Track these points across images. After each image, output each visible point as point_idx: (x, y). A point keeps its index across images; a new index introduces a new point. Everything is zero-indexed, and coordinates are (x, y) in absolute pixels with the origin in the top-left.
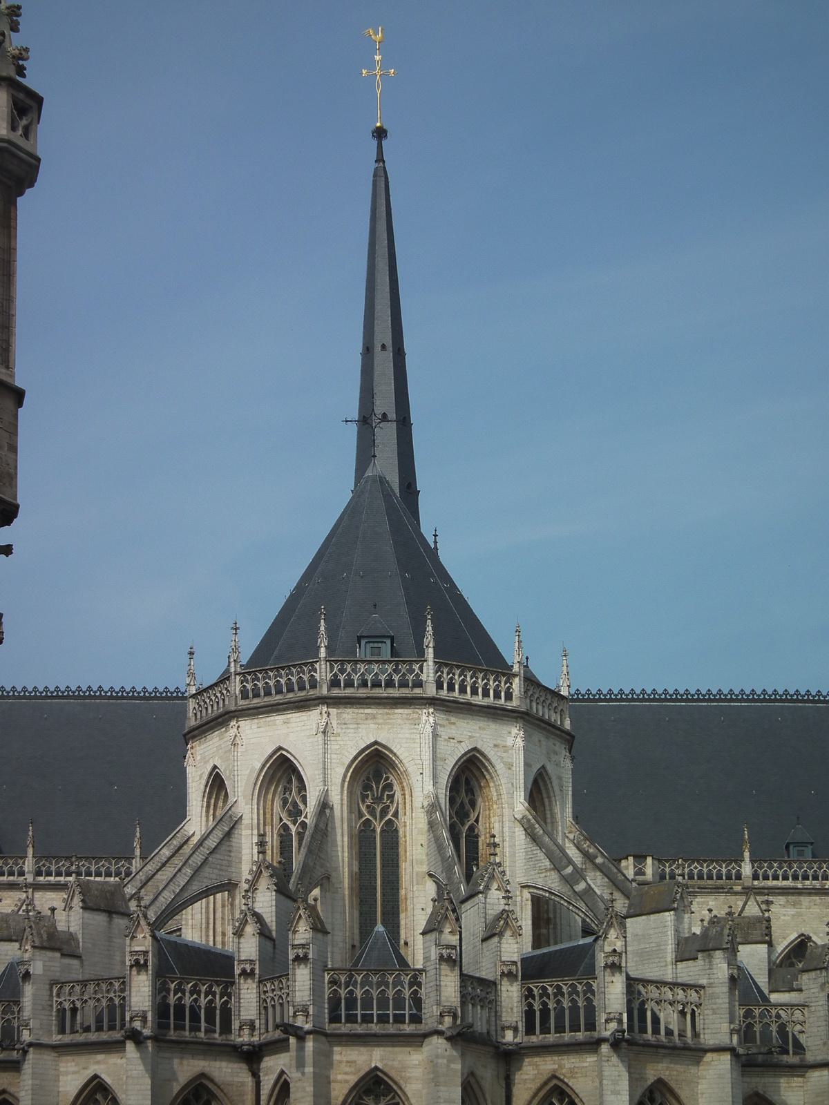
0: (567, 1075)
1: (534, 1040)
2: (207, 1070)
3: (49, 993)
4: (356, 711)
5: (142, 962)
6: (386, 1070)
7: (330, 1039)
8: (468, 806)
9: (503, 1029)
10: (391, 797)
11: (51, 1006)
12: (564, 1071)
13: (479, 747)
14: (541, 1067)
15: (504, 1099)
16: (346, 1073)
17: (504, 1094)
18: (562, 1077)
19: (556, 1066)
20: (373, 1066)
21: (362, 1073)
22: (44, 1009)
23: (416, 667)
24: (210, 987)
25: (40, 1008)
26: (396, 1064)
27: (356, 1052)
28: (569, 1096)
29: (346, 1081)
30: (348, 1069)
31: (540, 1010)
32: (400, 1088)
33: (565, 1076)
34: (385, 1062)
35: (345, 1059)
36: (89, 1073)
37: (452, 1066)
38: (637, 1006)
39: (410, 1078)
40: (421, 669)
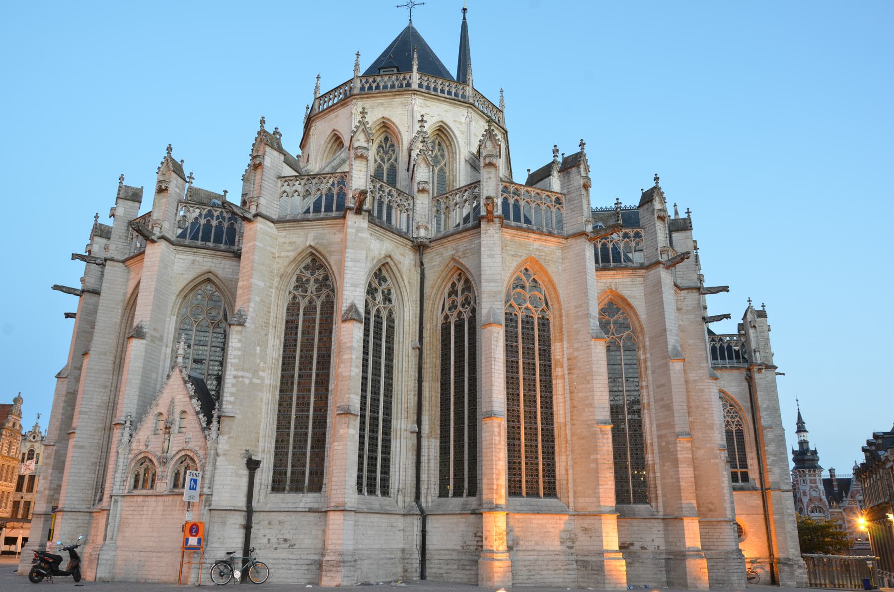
2: (213, 269)
5: (163, 187)
7: (278, 225)
8: (440, 157)
9: (418, 228)
10: (394, 151)
11: (127, 237)
12: (459, 254)
13: (444, 120)
14: (444, 255)
15: (419, 281)
16: (288, 251)
17: (419, 278)
19: (454, 252)
20: (308, 244)
21: (300, 250)
22: (120, 238)
23: (408, 77)
24: (221, 213)
25: (118, 237)
28: (465, 274)
29: (287, 257)
30: (290, 248)
32: (327, 260)
35: (288, 241)
37: (360, 234)
38: (513, 202)
40: (410, 78)
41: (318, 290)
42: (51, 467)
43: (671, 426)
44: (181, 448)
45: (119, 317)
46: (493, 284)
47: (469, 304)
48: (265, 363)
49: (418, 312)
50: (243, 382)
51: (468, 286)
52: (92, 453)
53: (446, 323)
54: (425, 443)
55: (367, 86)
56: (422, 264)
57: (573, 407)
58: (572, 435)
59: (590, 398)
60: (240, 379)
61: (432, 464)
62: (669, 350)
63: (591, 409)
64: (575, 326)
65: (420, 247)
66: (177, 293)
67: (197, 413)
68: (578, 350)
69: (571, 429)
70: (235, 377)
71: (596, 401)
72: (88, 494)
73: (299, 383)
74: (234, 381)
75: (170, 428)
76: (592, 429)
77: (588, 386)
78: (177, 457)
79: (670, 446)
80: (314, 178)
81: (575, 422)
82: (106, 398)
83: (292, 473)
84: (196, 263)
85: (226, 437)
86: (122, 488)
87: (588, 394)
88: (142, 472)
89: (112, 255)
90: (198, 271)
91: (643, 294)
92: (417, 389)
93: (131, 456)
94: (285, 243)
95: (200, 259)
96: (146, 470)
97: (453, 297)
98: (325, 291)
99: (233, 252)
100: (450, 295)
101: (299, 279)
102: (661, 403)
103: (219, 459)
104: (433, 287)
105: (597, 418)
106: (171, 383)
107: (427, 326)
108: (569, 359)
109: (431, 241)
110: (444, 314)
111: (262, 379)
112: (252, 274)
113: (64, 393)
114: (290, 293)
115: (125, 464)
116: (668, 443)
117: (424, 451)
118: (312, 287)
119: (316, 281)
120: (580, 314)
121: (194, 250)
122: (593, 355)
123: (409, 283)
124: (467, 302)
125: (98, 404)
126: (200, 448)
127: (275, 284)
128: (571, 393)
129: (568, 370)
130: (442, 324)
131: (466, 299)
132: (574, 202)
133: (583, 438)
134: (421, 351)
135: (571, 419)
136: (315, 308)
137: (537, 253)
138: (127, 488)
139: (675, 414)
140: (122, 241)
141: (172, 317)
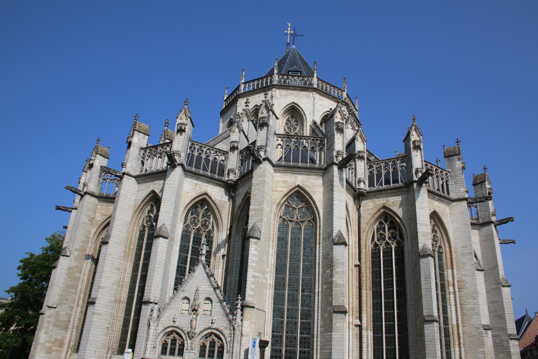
0: (391, 205)
1: (373, 189)
2: (209, 192)
3: (138, 153)
4: (286, 91)
6: (303, 187)
9: (359, 182)
16: (282, 187)
18: (388, 206)
19: (385, 201)
20: (297, 184)
21: (291, 188)
22: (135, 159)
26: (309, 184)
27: (288, 177)
29: (282, 191)
30: (283, 185)
31: (376, 174)
33: (390, 206)
34: (303, 183)
35: (282, 180)
36: (149, 190)
39: (316, 192)
42: (52, 325)
43: (505, 329)
44: (207, 327)
45: (130, 218)
46: (425, 227)
48: (268, 268)
49: (357, 240)
50: (258, 280)
52: (106, 320)
54: (364, 333)
55: (283, 80)
57: (463, 314)
58: (463, 333)
59: (476, 309)
60: (257, 279)
61: (370, 349)
62: (501, 279)
63: (478, 317)
64: (462, 260)
66: (185, 206)
67: (221, 302)
68: (465, 275)
69: (463, 330)
70: (254, 277)
71: (481, 312)
72: (101, 352)
73: (289, 285)
74: (253, 280)
75: (196, 310)
76: (479, 330)
77: (474, 301)
78: (204, 333)
79: (504, 343)
80: (293, 138)
81: (465, 325)
82: (118, 278)
83: (286, 351)
84: (198, 186)
85: (248, 322)
86: (152, 353)
87: (475, 306)
88: (169, 342)
89: (128, 171)
90: (199, 192)
91: (479, 241)
92: (358, 294)
93: (160, 328)
94: (279, 181)
95: (200, 183)
96: (174, 341)
99: (223, 182)
100: (378, 230)
102: (496, 313)
103: (243, 338)
104: (367, 224)
105: (482, 323)
106: (196, 276)
107: (363, 251)
108: (458, 282)
110: (374, 242)
111: (266, 279)
112: (263, 201)
113: (67, 267)
114: (281, 217)
115: (155, 334)
116: (501, 341)
117: (364, 339)
120: (466, 252)
121: (198, 176)
122: (477, 280)
123: (352, 219)
125: (113, 282)
126: (226, 328)
127: (274, 210)
128: (461, 304)
129: (458, 289)
130: (372, 250)
132: (457, 178)
133: (472, 336)
134: (359, 266)
135: (462, 323)
137: (438, 209)
138: (157, 353)
139: (507, 322)
140: (136, 161)
141: (180, 224)
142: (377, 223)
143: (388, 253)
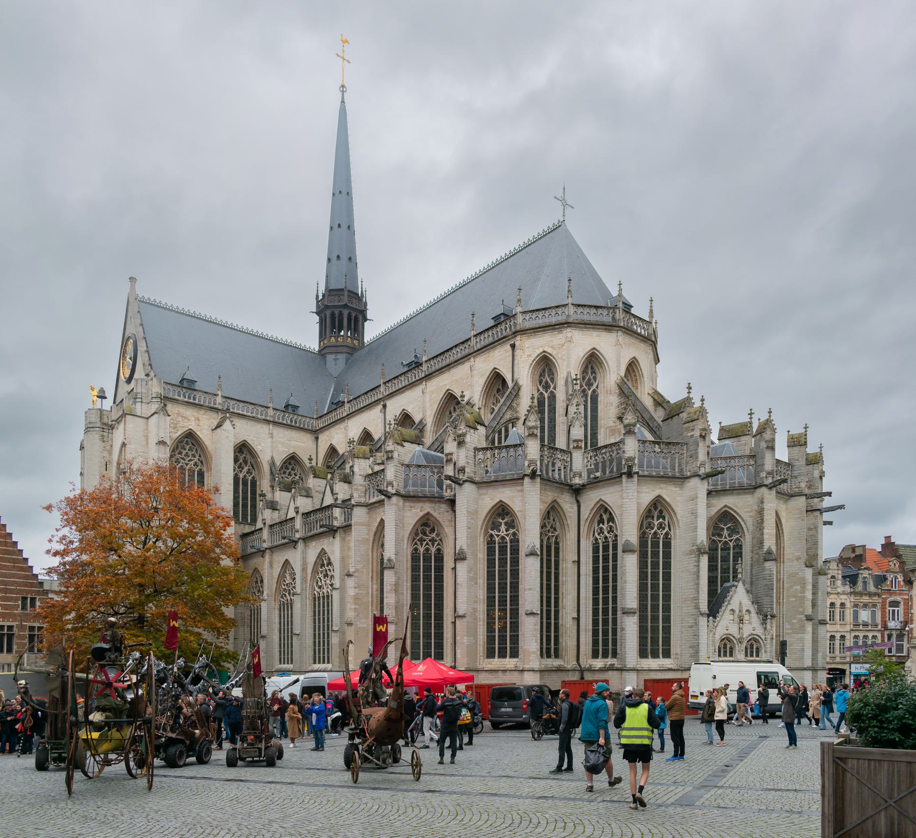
9: (574, 476)
41: (507, 531)
47: (613, 532)
51: (611, 519)
53: (596, 543)
56: (578, 502)
65: (577, 491)
97: (601, 525)
98: (511, 531)
100: (598, 525)
101: (493, 523)
104: (586, 521)
109: (584, 485)
118: (503, 528)
119: (506, 524)
124: (611, 530)
131: (611, 527)
136: (506, 543)
142: (598, 516)
143: (606, 548)
